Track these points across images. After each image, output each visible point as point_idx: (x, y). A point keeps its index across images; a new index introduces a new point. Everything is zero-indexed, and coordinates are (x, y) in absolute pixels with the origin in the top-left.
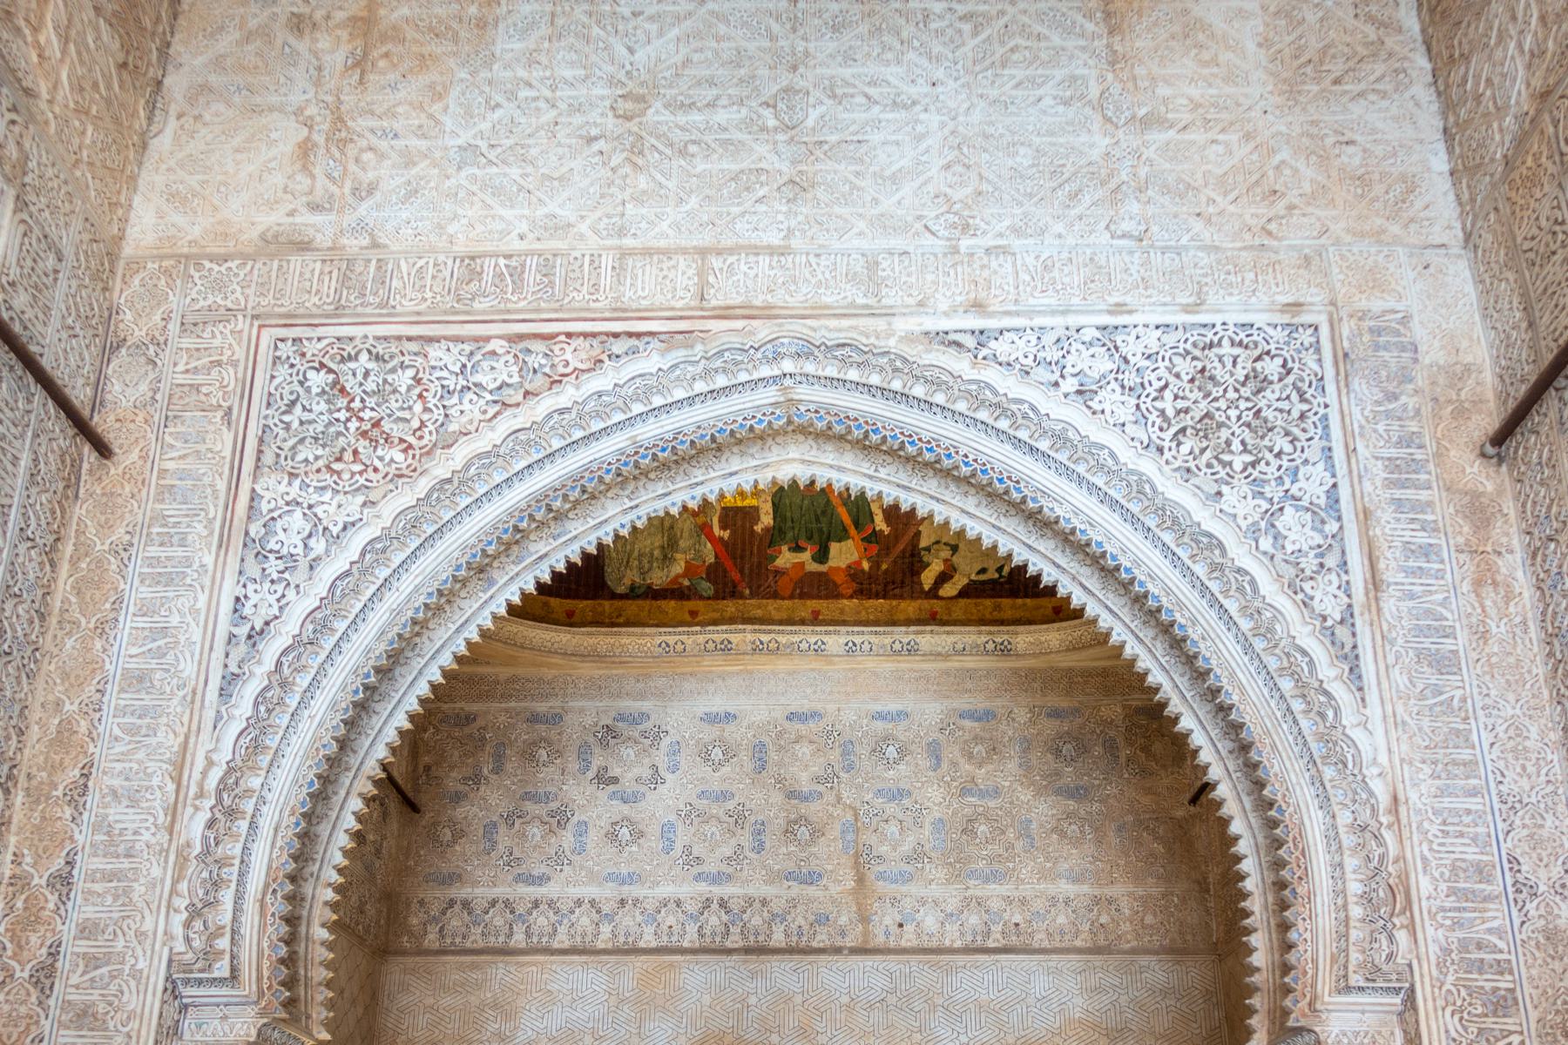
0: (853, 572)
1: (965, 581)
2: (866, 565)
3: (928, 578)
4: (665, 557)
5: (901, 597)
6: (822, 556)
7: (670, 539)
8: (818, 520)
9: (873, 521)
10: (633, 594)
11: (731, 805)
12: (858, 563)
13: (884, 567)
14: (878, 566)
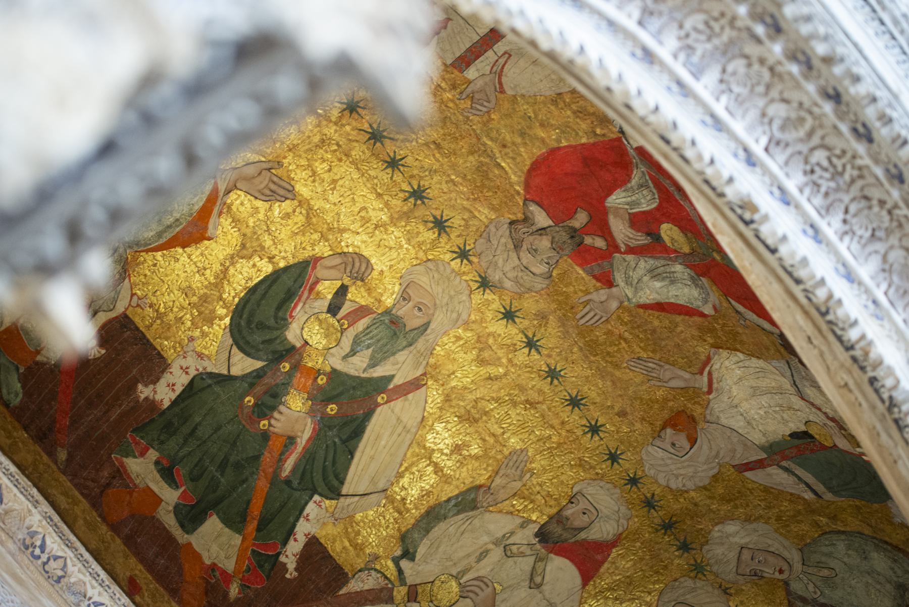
2: (234, 591)
9: (285, 542)
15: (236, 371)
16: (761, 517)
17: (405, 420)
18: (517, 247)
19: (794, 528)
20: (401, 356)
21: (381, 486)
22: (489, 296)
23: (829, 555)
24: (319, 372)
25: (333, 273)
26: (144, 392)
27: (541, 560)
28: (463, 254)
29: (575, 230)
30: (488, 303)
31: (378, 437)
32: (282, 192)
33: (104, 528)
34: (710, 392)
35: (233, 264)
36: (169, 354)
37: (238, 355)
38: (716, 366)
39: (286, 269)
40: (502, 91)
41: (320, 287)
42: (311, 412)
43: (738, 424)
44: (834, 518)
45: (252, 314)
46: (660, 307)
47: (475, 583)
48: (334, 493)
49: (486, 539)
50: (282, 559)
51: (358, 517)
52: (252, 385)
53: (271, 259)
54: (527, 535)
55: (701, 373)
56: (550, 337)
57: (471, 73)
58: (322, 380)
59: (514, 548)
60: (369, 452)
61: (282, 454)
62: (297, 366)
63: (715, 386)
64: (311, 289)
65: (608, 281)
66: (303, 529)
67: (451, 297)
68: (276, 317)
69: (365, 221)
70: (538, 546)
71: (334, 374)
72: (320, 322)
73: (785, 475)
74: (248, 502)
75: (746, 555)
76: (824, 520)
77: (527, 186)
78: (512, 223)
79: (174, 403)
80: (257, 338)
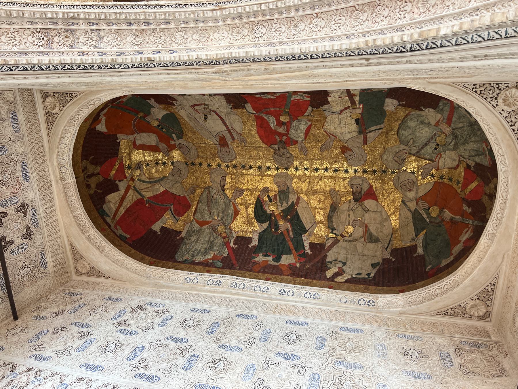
0: (291, 267)
1: (350, 277)
2: (298, 265)
3: (329, 274)
4: (206, 252)
5: (314, 279)
6: (278, 259)
7: (210, 246)
8: (278, 245)
9: (304, 248)
10: (185, 262)
11: (183, 345)
12: (295, 264)
13: (307, 267)
14: (304, 266)
15: (265, 228)
16: (384, 147)
17: (304, 206)
18: (281, 156)
19: (392, 141)
20: (290, 196)
21: (313, 221)
22: (290, 169)
23: (406, 137)
24: (280, 213)
25: (264, 195)
26: (250, 246)
27: (362, 205)
28: (277, 168)
29: (280, 141)
30: (291, 171)
31: (303, 214)
32: (242, 192)
33: (255, 274)
34: (336, 138)
35: (247, 211)
36: (251, 236)
37: (263, 225)
38: (329, 131)
39: (256, 203)
40: (241, 134)
41: (264, 200)
42: (286, 221)
43: (348, 136)
44: (392, 130)
45: (259, 216)
46: (307, 133)
47: (354, 222)
48: (306, 231)
49: (346, 212)
50: (306, 252)
51: (315, 231)
52: (271, 227)
53: (252, 204)
54: (353, 204)
55: (329, 136)
56: (306, 164)
57: (236, 138)
58: (282, 214)
59: (354, 208)
60: (304, 218)
61: (288, 233)
62: (275, 217)
63: (334, 135)
64: (263, 201)
65: (296, 142)
66: (306, 243)
67: (285, 177)
68: (263, 212)
69: (258, 181)
70: (358, 203)
71: (283, 211)
72: (271, 205)
73: (371, 134)
74: (289, 247)
75: (395, 158)
76: (393, 132)
77: (267, 145)
78: (275, 153)
79: (258, 243)
80: (263, 218)
